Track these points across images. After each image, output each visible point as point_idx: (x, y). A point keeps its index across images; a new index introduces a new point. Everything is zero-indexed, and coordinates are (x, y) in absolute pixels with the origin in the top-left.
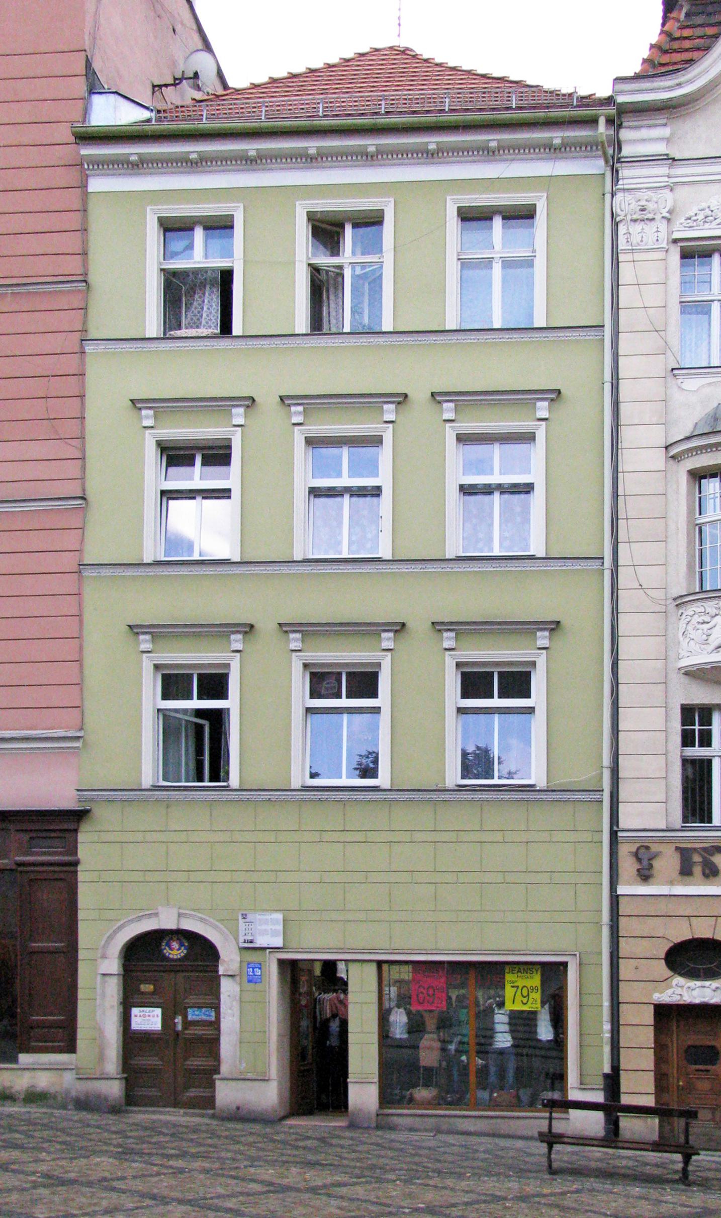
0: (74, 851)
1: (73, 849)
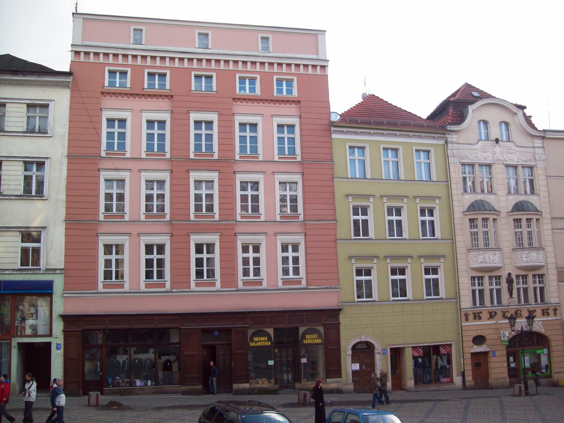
0: (339, 320)
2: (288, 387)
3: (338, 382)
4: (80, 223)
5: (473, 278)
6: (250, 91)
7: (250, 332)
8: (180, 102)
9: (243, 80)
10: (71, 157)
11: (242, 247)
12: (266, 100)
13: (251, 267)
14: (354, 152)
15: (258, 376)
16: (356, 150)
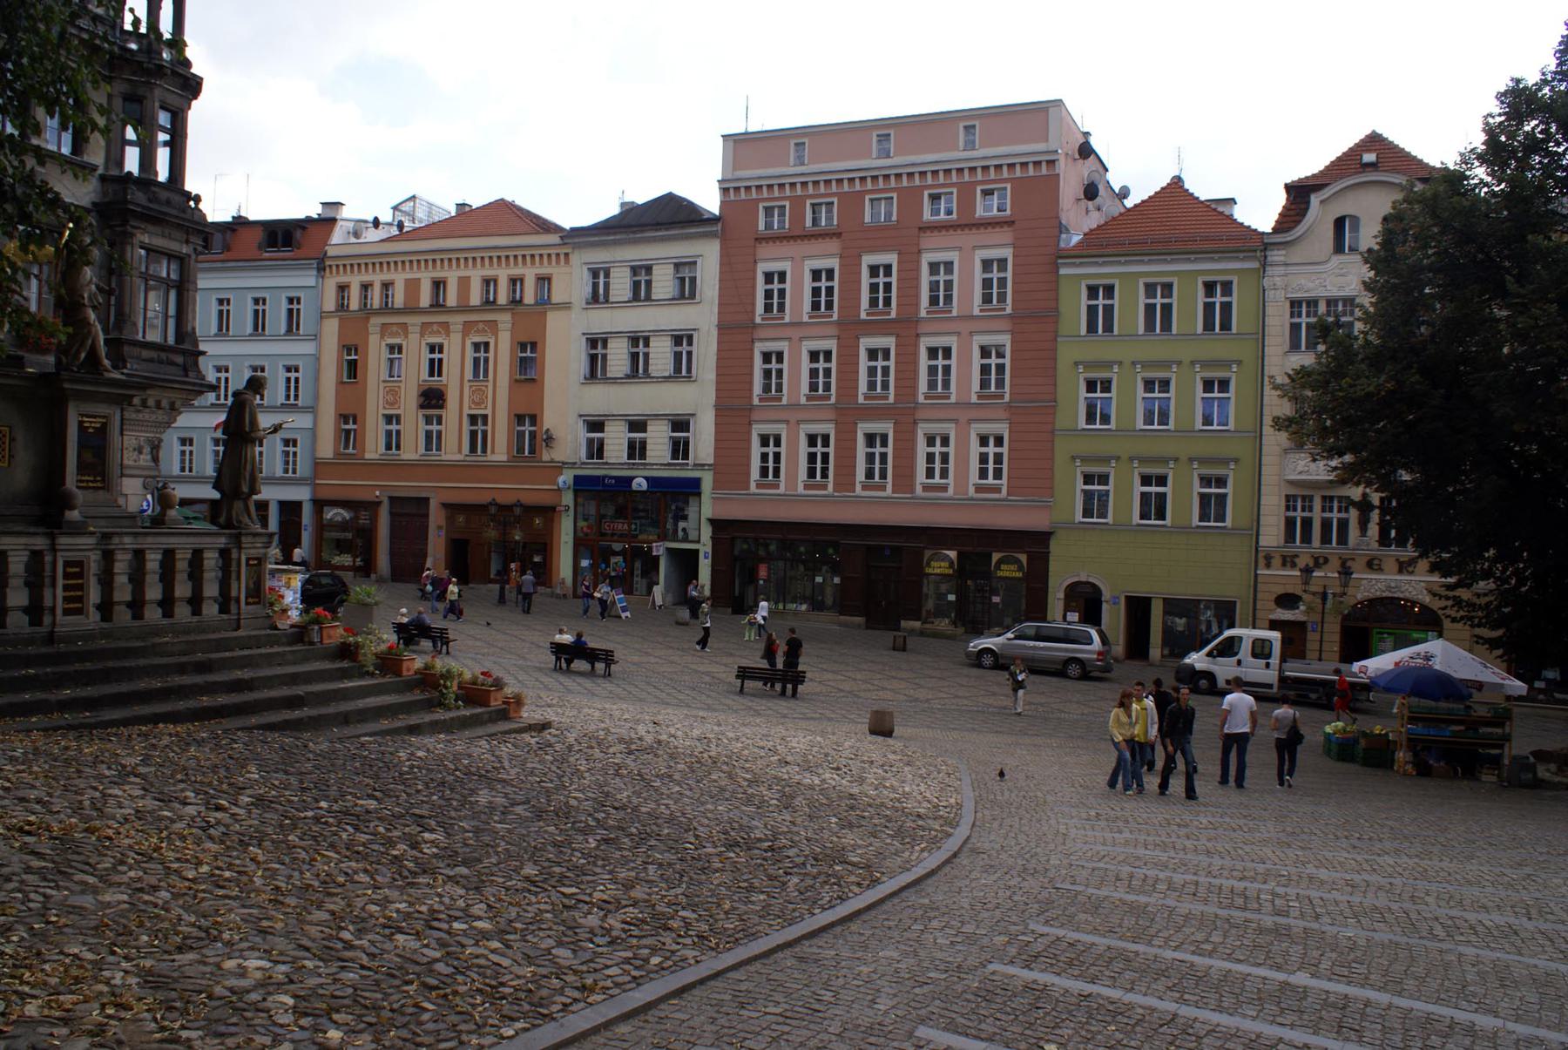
1: (1048, 547)
4: (733, 411)
5: (1288, 498)
8: (851, 237)
9: (935, 198)
10: (722, 328)
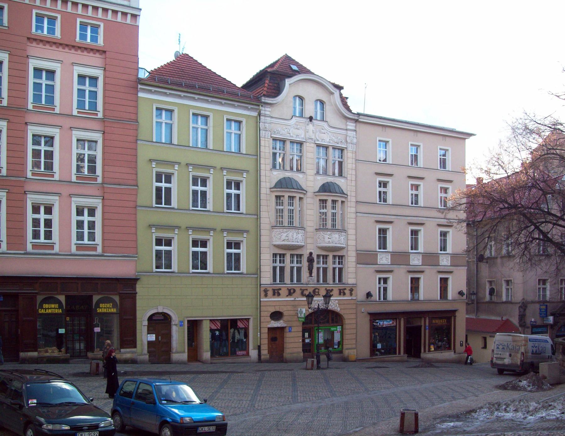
2: (79, 356)
3: (133, 353)
5: (275, 255)
6: (48, 33)
7: (40, 298)
11: (33, 206)
12: (67, 45)
13: (42, 229)
14: (161, 114)
15: (48, 344)
16: (164, 112)
